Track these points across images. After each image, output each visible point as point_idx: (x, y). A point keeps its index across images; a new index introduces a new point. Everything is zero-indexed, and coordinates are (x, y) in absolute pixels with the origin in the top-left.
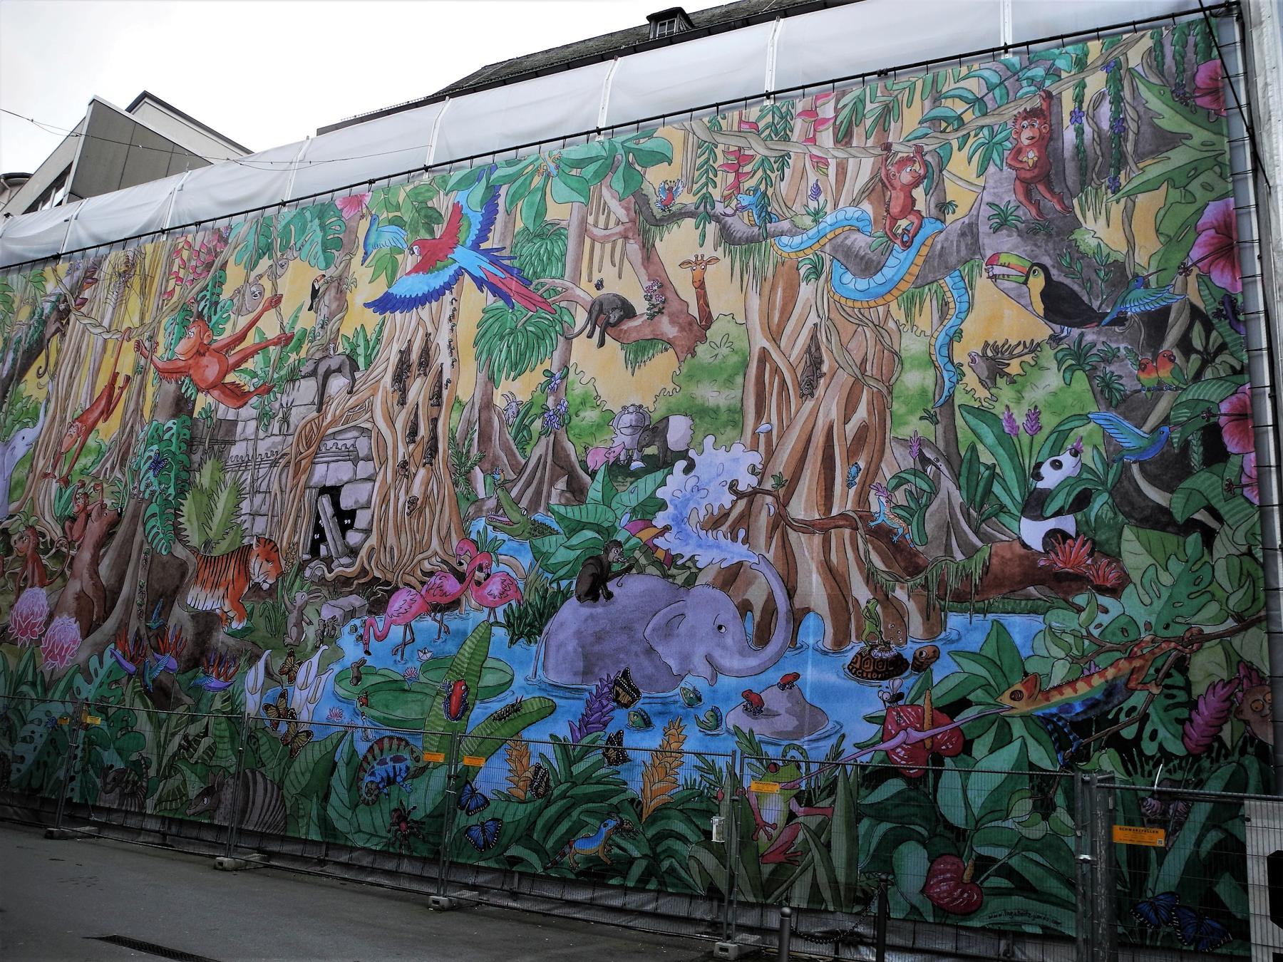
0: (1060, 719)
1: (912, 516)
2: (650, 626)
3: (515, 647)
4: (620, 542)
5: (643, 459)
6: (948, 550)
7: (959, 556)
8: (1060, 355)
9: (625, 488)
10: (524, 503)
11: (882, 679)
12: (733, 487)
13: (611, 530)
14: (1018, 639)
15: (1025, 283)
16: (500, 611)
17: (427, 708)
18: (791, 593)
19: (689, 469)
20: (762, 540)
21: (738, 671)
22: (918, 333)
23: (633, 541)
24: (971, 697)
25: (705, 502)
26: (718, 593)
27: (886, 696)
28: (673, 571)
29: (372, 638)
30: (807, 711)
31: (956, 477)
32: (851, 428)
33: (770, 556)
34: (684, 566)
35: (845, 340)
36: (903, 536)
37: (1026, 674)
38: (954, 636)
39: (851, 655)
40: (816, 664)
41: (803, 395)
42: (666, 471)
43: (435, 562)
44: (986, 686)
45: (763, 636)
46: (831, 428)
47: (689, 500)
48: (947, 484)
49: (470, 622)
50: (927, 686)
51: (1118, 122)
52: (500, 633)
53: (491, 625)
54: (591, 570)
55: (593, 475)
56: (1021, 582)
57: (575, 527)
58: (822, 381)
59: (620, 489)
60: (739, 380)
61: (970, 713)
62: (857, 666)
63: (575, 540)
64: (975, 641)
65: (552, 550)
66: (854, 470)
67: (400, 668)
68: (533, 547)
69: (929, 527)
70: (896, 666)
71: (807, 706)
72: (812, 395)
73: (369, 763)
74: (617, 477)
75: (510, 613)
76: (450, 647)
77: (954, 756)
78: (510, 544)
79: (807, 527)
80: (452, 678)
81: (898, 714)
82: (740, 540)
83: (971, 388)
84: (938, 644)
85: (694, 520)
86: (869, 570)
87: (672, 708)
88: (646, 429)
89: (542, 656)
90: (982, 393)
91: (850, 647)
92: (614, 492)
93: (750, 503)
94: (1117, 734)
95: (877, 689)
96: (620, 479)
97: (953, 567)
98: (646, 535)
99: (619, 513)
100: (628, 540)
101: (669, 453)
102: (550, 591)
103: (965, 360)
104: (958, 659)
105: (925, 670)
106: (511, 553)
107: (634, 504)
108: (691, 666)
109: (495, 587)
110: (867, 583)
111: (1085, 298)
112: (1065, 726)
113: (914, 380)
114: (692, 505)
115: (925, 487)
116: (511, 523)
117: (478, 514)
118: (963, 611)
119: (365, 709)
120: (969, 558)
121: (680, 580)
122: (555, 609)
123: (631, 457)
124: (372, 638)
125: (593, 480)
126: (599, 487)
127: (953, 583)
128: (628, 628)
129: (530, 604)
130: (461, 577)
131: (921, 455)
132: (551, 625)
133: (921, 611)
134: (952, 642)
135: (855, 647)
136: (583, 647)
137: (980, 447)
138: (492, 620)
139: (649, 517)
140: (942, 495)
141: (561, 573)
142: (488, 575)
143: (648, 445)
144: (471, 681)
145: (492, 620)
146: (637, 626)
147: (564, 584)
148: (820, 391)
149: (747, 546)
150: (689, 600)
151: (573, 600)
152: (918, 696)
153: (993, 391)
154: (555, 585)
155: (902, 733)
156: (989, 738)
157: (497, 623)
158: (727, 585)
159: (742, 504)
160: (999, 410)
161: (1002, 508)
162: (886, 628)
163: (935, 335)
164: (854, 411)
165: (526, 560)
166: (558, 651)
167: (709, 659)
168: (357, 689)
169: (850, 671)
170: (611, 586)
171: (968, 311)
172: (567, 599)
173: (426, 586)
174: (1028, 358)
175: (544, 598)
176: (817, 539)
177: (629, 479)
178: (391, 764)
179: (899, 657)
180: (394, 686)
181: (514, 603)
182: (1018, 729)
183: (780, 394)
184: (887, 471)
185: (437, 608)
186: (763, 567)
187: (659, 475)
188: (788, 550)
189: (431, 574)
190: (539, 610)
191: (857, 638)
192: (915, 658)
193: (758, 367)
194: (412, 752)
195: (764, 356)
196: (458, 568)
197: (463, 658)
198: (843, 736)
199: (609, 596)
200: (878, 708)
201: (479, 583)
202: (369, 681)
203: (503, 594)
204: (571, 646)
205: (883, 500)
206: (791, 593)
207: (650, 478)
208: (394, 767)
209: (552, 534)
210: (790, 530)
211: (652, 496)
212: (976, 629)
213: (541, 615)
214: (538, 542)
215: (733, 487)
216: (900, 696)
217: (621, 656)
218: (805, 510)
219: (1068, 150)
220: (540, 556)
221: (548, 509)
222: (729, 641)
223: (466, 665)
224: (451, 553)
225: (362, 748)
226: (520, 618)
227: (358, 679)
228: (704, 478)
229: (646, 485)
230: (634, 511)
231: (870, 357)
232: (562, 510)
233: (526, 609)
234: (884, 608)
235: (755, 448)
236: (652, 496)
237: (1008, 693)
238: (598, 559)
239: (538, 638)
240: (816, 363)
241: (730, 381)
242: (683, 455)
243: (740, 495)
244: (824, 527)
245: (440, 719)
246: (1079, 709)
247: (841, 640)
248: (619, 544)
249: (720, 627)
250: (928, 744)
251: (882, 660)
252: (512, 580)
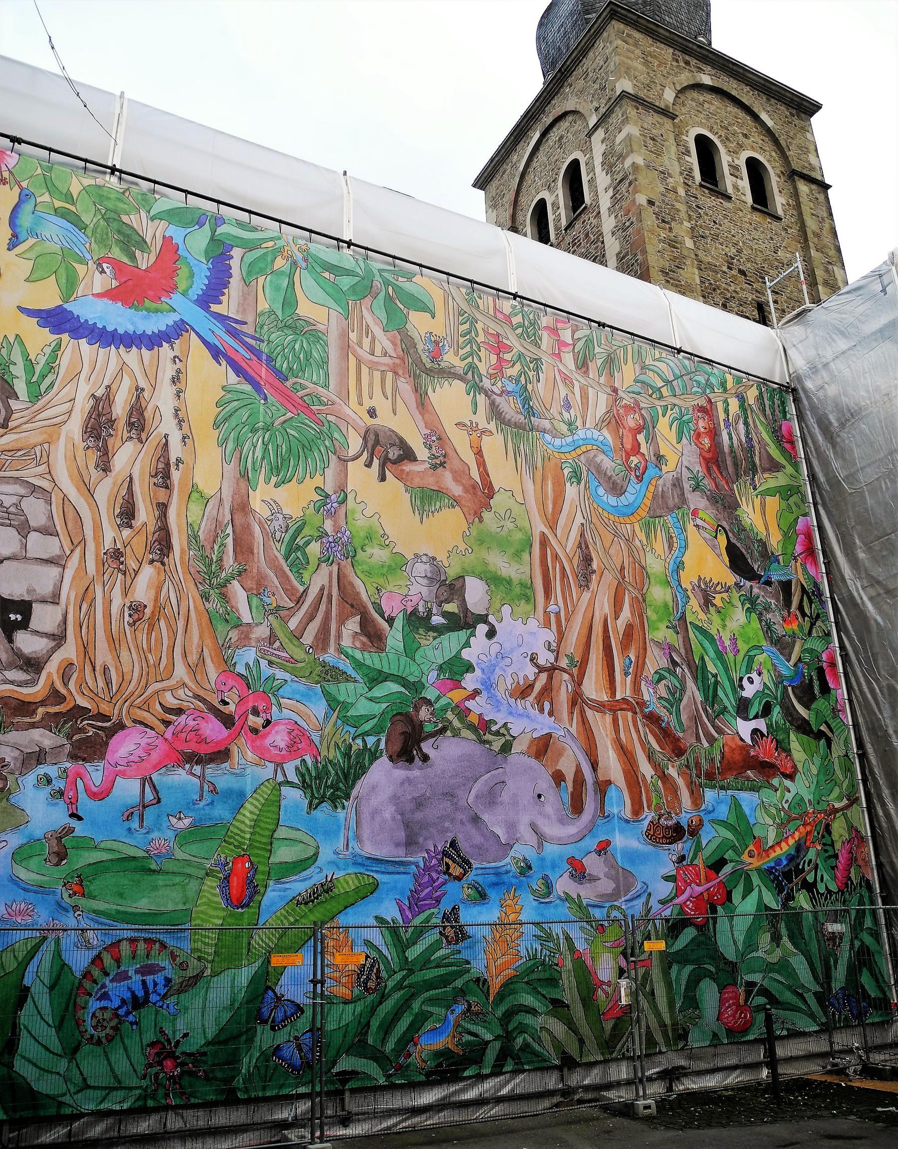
0: (776, 870)
1: (672, 707)
2: (473, 792)
3: (318, 814)
4: (429, 701)
5: (445, 614)
6: (698, 739)
7: (706, 744)
8: (742, 598)
9: (427, 643)
10: (308, 638)
12: (533, 659)
13: (418, 685)
14: (747, 810)
15: (716, 537)
16: (290, 768)
17: (191, 894)
18: (594, 766)
19: (491, 634)
20: (565, 715)
21: (559, 839)
22: (656, 555)
23: (443, 701)
24: (726, 856)
25: (510, 671)
26: (533, 762)
27: (674, 858)
28: (488, 737)
29: (82, 795)
30: (621, 874)
31: (695, 678)
32: (621, 623)
33: (573, 730)
34: (497, 733)
35: (607, 545)
36: (668, 723)
37: (755, 838)
38: (710, 808)
39: (646, 823)
40: (622, 831)
41: (581, 586)
42: (469, 631)
43: (183, 697)
44: (733, 847)
45: (577, 807)
46: (606, 620)
47: (495, 666)
48: (690, 683)
49: (249, 780)
50: (698, 848)
51: (749, 440)
52: (293, 796)
53: (280, 784)
54: (401, 728)
55: (390, 621)
56: (742, 767)
57: (376, 678)
58: (594, 577)
59: (423, 642)
60: (526, 556)
61: (727, 869)
63: (378, 691)
64: (723, 812)
65: (350, 701)
66: (627, 661)
67: (139, 838)
68: (326, 694)
69: (684, 718)
70: (676, 833)
71: (620, 870)
72: (587, 586)
73: (95, 982)
74: (418, 629)
75: (304, 770)
76: (221, 811)
77: (723, 904)
78: (295, 685)
79: (600, 707)
80: (227, 853)
82: (546, 711)
83: (694, 611)
84: (702, 814)
85: (502, 688)
87: (505, 878)
88: (443, 583)
89: (353, 824)
90: (702, 616)
91: (644, 816)
92: (416, 645)
93: (550, 678)
94: (805, 880)
95: (667, 852)
96: (421, 631)
97: (703, 751)
98: (456, 696)
99: (425, 668)
100: (438, 698)
101: (469, 615)
102: (354, 749)
103: (689, 587)
104: (715, 826)
105: (696, 835)
106: (298, 697)
107: (440, 661)
108: (518, 835)
109: (279, 738)
111: (749, 560)
112: (779, 875)
113: (659, 594)
114: (498, 672)
115: (677, 685)
116: (293, 660)
117: (244, 641)
118: (714, 787)
119: (82, 902)
120: (712, 745)
121: (497, 746)
122: (362, 770)
123: (430, 610)
124: (82, 795)
125: (391, 626)
126: (399, 636)
127: (705, 766)
128: (450, 795)
129: (330, 762)
130: (227, 721)
131: (671, 657)
132: (361, 787)
133: (688, 787)
134: (710, 812)
135: (649, 816)
136: (402, 814)
137: (706, 658)
138: (280, 778)
139: (457, 677)
140: (688, 693)
141: (367, 726)
142: (268, 723)
143: (448, 601)
144: (257, 855)
145: (280, 778)
146: (459, 792)
147: (371, 741)
148: (593, 585)
149: (553, 718)
150: (508, 768)
151: (384, 761)
153: (708, 615)
154: (359, 741)
156: (740, 888)
157: (288, 783)
158: (540, 755)
159: (544, 676)
160: (714, 632)
161: (725, 708)
162: (667, 800)
163: (668, 560)
164: (621, 609)
165: (319, 708)
166: (373, 818)
167: (534, 827)
168: (60, 872)
170: (426, 747)
171: (686, 547)
172: (377, 758)
173: (171, 728)
174: (725, 595)
175: (347, 755)
176: (608, 718)
177: (431, 633)
178: (139, 977)
180: (133, 864)
181: (309, 759)
182: (756, 880)
183: (562, 580)
184: (651, 667)
185: (193, 759)
186: (569, 740)
187: (463, 634)
188: (587, 726)
189: (179, 711)
190: (343, 770)
192: (689, 826)
193: (541, 549)
194: (173, 956)
195: (544, 542)
196: (222, 708)
197: (242, 827)
198: (650, 894)
199: (425, 758)
200: (670, 869)
201: (255, 731)
202: (82, 859)
203: (293, 749)
204: (388, 813)
205: (651, 691)
206: (594, 766)
207: (454, 635)
208: (144, 982)
209: (347, 681)
210: (586, 708)
211: (458, 656)
212: (722, 802)
213: (346, 776)
214: (332, 688)
215: (533, 659)
217: (447, 824)
218: (596, 692)
219: (726, 449)
220: (333, 703)
221: (340, 650)
222: (549, 809)
223: (248, 836)
224: (208, 687)
225: (79, 960)
226: (318, 777)
227: (61, 855)
228: (507, 646)
229: (452, 642)
230: (441, 668)
231: (626, 565)
232: (358, 655)
233: (325, 767)
234: (664, 783)
235: (547, 625)
236: (458, 656)
237: (746, 852)
238: (407, 715)
239: (346, 803)
240: (587, 560)
241: (517, 554)
242: (484, 619)
243: (541, 669)
244: (613, 707)
245: (216, 909)
246: (785, 863)
247: (637, 810)
248: (428, 702)
249: (539, 796)
250: (706, 896)
251: (667, 827)
252: (303, 731)
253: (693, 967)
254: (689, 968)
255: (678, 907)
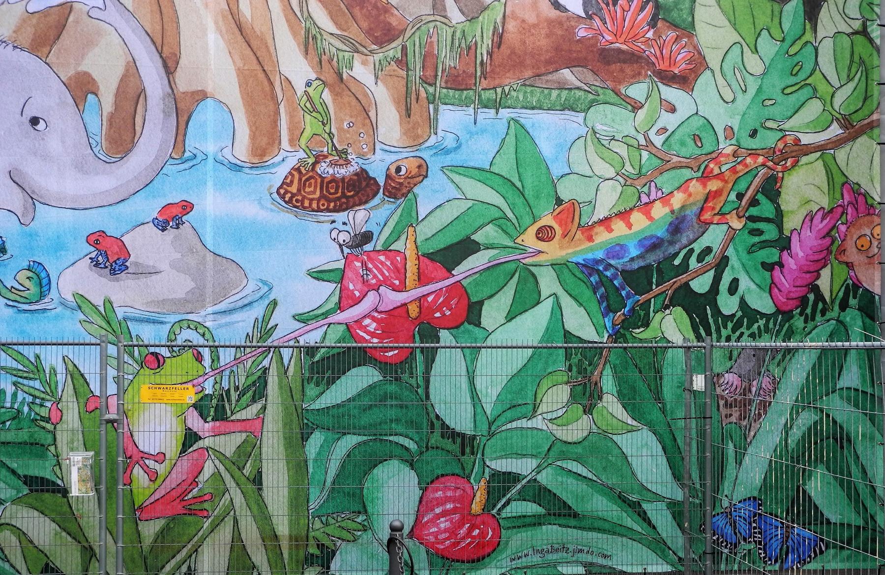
11: (336, 210)
39: (282, 172)
62: (294, 189)
81: (364, 264)
86: (308, 31)
91: (278, 159)
95: (328, 226)
110: (306, 52)
152: (396, 236)
155: (372, 295)
162: (340, 129)
169: (282, 197)
179: (363, 176)
191: (292, 142)
192: (388, 177)
216: (367, 237)
234: (336, 95)
251: (334, 180)
253: (361, 439)
254: (350, 441)
255: (343, 328)
